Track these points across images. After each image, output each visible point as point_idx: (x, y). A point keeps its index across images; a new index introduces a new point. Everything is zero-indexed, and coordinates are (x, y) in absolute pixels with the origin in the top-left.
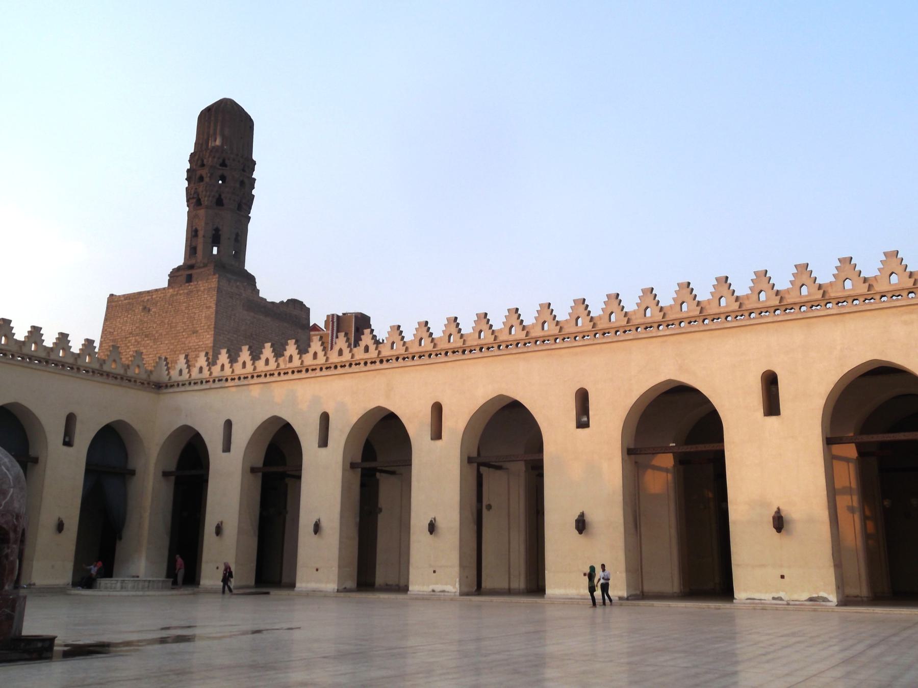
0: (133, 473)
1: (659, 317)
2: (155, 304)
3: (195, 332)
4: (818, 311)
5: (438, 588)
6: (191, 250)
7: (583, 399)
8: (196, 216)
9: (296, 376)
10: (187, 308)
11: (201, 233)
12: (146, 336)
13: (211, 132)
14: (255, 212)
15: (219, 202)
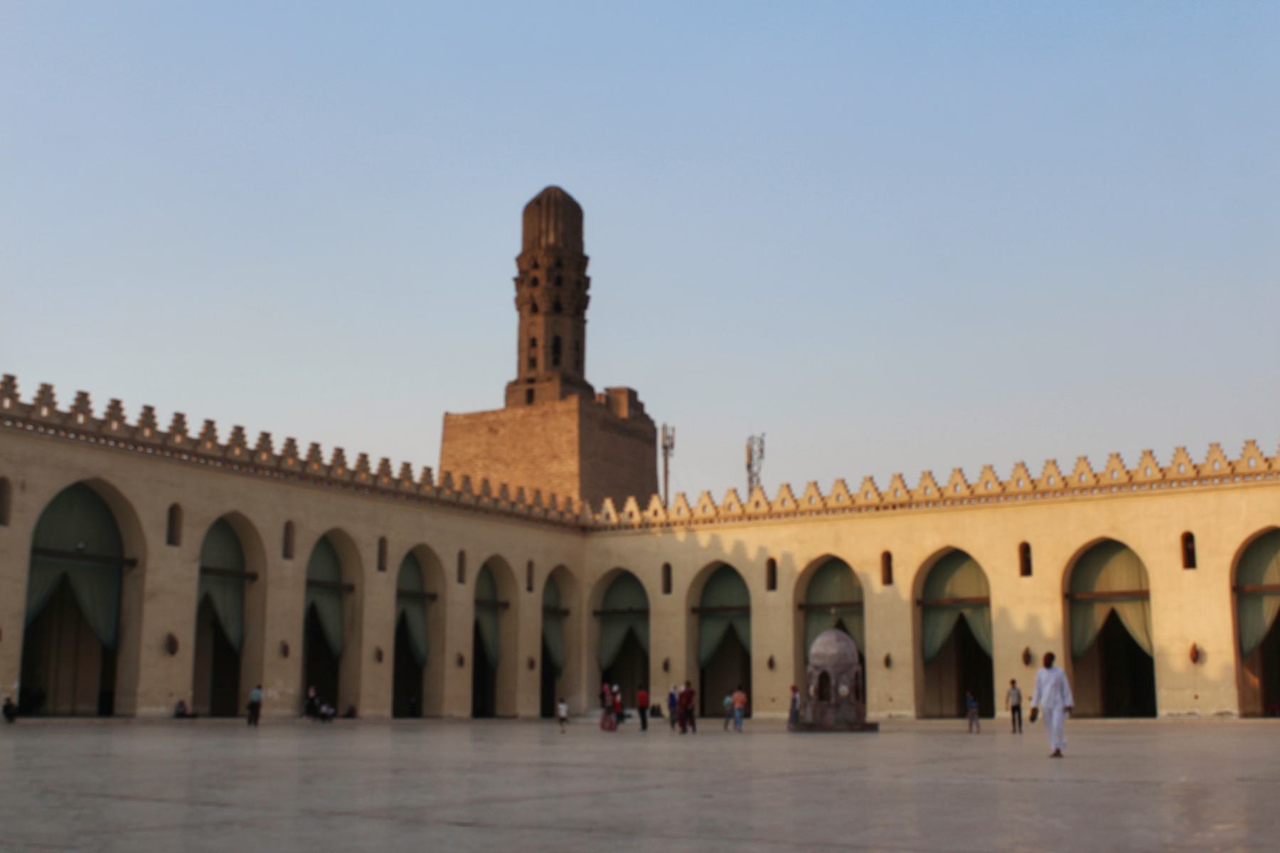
0: (566, 613)
1: (1092, 482)
2: (503, 424)
3: (555, 457)
4: (1228, 484)
5: (894, 713)
6: (528, 360)
7: (1025, 550)
8: (533, 324)
9: (737, 523)
10: (544, 429)
11: (541, 343)
12: (498, 460)
13: (544, 226)
14: (592, 314)
15: (557, 308)
